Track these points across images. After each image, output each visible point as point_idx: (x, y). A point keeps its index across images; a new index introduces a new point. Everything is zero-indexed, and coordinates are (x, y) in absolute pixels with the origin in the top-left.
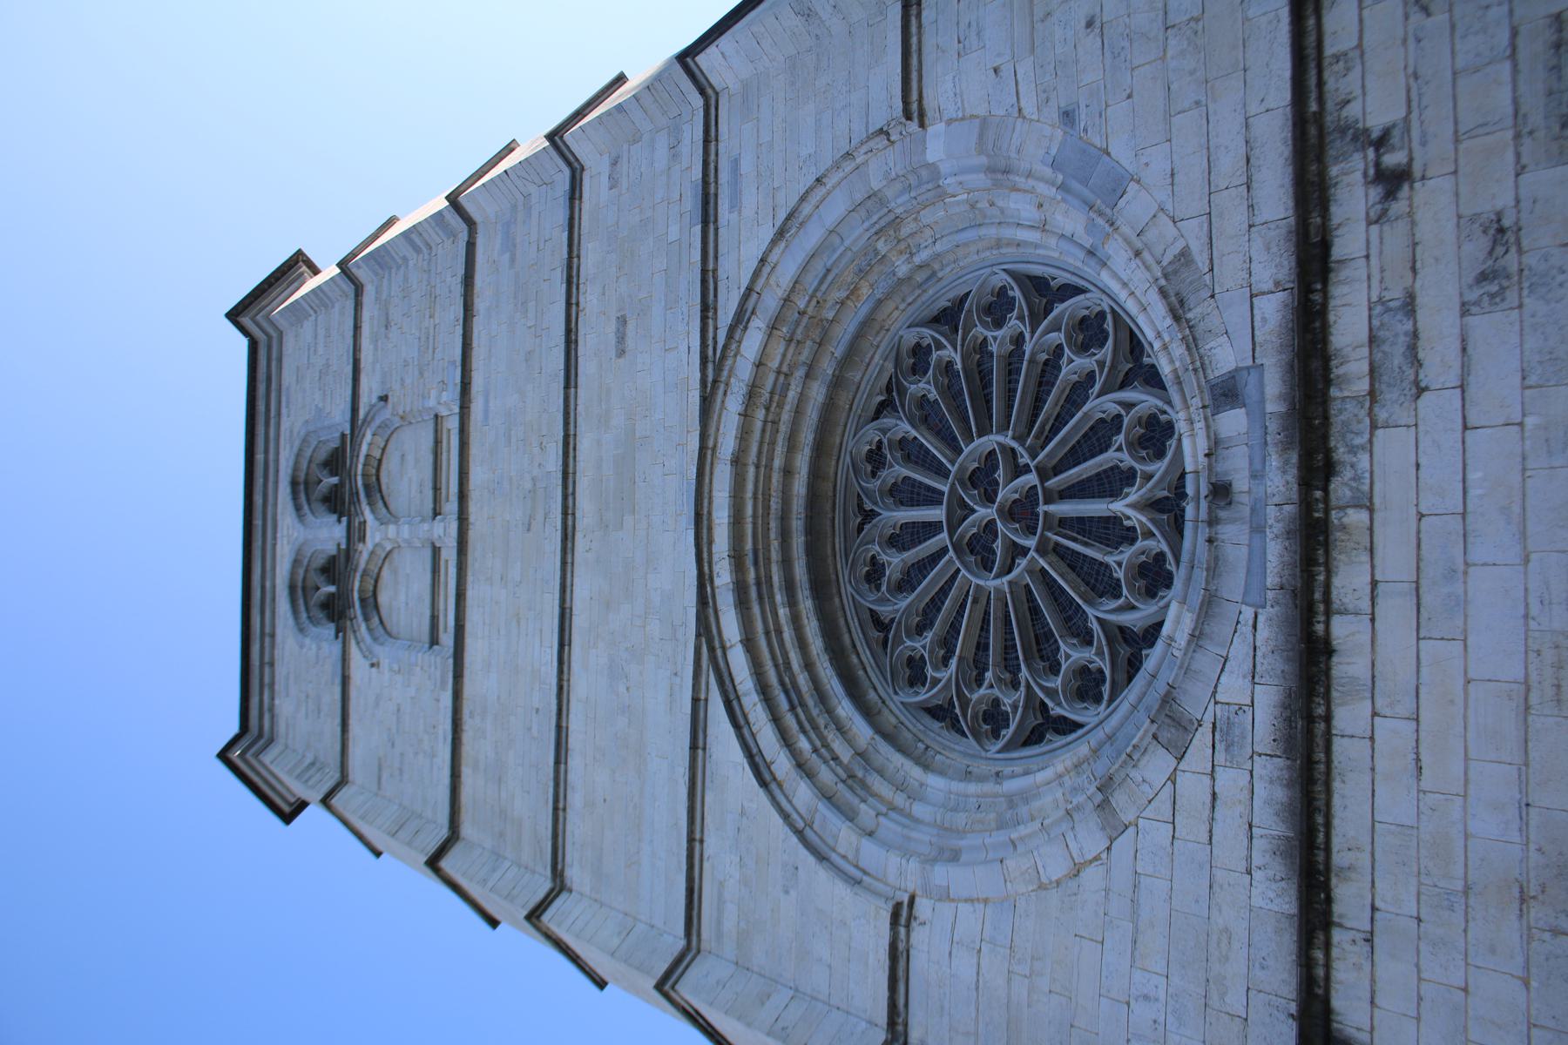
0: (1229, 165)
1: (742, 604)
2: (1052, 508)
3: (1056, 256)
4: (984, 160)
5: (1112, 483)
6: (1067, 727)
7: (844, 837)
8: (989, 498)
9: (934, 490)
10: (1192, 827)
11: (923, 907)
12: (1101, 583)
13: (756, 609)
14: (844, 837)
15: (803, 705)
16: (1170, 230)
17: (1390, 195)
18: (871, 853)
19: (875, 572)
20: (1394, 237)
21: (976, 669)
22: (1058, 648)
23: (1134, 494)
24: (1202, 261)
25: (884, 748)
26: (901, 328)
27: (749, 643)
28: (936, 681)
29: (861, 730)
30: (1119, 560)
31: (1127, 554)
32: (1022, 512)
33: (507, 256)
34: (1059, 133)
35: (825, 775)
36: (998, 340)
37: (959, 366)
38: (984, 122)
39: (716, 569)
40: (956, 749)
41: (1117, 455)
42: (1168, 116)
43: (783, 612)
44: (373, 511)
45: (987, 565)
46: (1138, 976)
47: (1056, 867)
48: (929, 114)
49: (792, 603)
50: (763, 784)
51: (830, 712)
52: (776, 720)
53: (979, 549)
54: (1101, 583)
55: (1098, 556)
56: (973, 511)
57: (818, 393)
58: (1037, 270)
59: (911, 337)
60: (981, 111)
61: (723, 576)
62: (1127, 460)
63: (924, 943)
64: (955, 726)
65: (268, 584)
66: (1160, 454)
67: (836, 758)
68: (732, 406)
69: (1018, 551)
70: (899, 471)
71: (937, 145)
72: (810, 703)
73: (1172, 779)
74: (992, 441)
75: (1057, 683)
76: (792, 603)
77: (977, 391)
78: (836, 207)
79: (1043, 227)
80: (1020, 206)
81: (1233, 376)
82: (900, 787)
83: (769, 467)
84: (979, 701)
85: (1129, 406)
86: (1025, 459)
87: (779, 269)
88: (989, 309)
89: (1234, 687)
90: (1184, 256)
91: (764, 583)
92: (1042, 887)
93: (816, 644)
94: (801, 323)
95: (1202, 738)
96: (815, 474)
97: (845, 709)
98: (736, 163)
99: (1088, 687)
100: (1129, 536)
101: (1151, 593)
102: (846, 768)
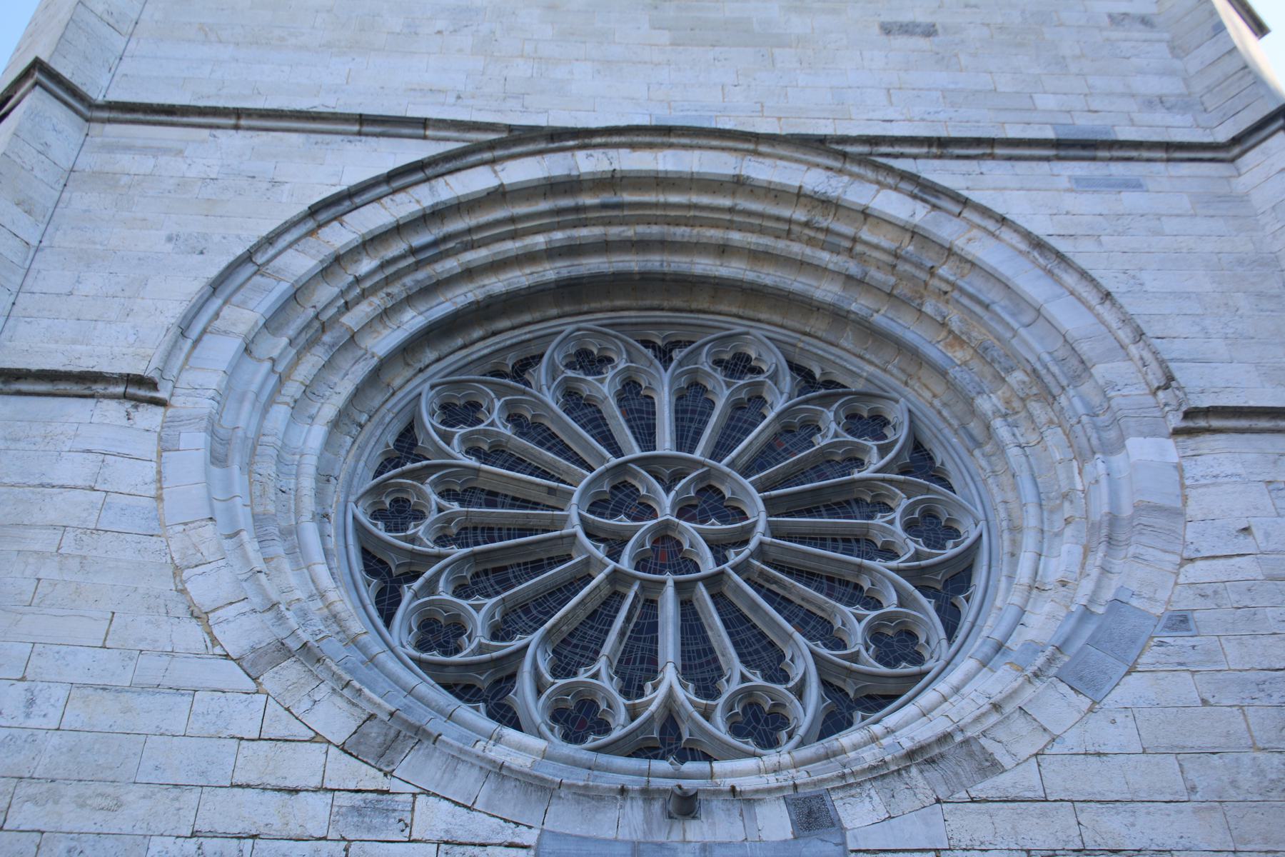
1: (551, 187)
2: (670, 591)
3: (996, 603)
4: (1126, 511)
5: (701, 668)
6: (387, 605)
7: (245, 314)
8: (684, 511)
9: (695, 441)
10: (256, 762)
11: (150, 417)
12: (571, 651)
13: (543, 206)
14: (245, 314)
15: (418, 265)
16: (1025, 750)
18: (221, 350)
19: (590, 362)
22: (488, 596)
23: (685, 696)
24: (984, 788)
25: (360, 371)
26: (908, 401)
27: (500, 195)
28: (447, 438)
29: (385, 341)
30: (600, 675)
31: (609, 685)
32: (666, 552)
34: (1158, 610)
35: (326, 293)
36: (890, 525)
37: (857, 475)
38: (1177, 513)
39: (598, 153)
40: (358, 465)
41: (736, 674)
42: (1177, 751)
43: (540, 241)
45: (598, 506)
46: (60, 692)
47: (202, 589)
48: (1191, 443)
49: (552, 253)
50: (314, 211)
51: (409, 300)
52: (398, 229)
53: (618, 496)
54: (571, 651)
55: (607, 649)
56: (668, 490)
57: (827, 291)
58: (979, 579)
59: (896, 413)
60: (1192, 510)
61: (588, 163)
62: (730, 688)
63: (104, 418)
64: (389, 462)
66: (736, 730)
67: (347, 307)
69: (615, 544)
70: (722, 394)
71: (1150, 453)
72: (421, 275)
73: (317, 738)
74: (759, 516)
75: (444, 593)
76: (552, 253)
77: (824, 497)
78: (1069, 317)
79: (1035, 586)
80: (1063, 558)
81: (835, 824)
82: (309, 391)
83: (730, 225)
84: (421, 494)
85: (800, 691)
86: (734, 557)
87: (993, 242)
88: (929, 514)
90: (992, 767)
91: (578, 216)
92: (177, 570)
93: (498, 284)
94: (919, 269)
95: (370, 777)
97: (413, 320)
98: (1136, 185)
99: (438, 633)
100: (632, 688)
101: (558, 715)
102: (334, 320)
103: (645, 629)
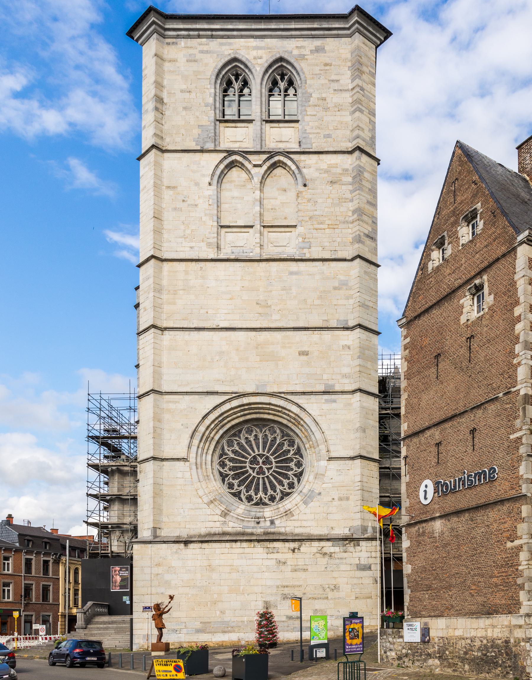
0: (304, 524)
7: (196, 442)
8: (263, 463)
10: (211, 518)
14: (196, 442)
17: (292, 550)
18: (194, 449)
19: (249, 432)
20: (286, 550)
21: (231, 460)
24: (292, 519)
25: (214, 443)
27: (232, 409)
30: (252, 492)
31: (253, 494)
32: (261, 472)
33: (337, 284)
36: (292, 465)
37: (288, 456)
38: (324, 475)
41: (270, 492)
42: (314, 513)
43: (239, 414)
44: (266, 171)
46: (187, 510)
47: (201, 493)
49: (241, 416)
51: (220, 428)
53: (254, 461)
57: (285, 422)
60: (326, 475)
61: (245, 400)
63: (182, 463)
65: (235, 33)
68: (281, 403)
72: (221, 424)
76: (241, 416)
77: (284, 461)
80: (311, 478)
81: (275, 524)
85: (277, 494)
89: (231, 524)
90: (293, 515)
93: (233, 423)
94: (297, 420)
95: (223, 519)
96: (269, 420)
97: (221, 432)
98: (335, 401)
99: (231, 486)
100: (256, 494)
101: (247, 498)
103: (258, 484)
